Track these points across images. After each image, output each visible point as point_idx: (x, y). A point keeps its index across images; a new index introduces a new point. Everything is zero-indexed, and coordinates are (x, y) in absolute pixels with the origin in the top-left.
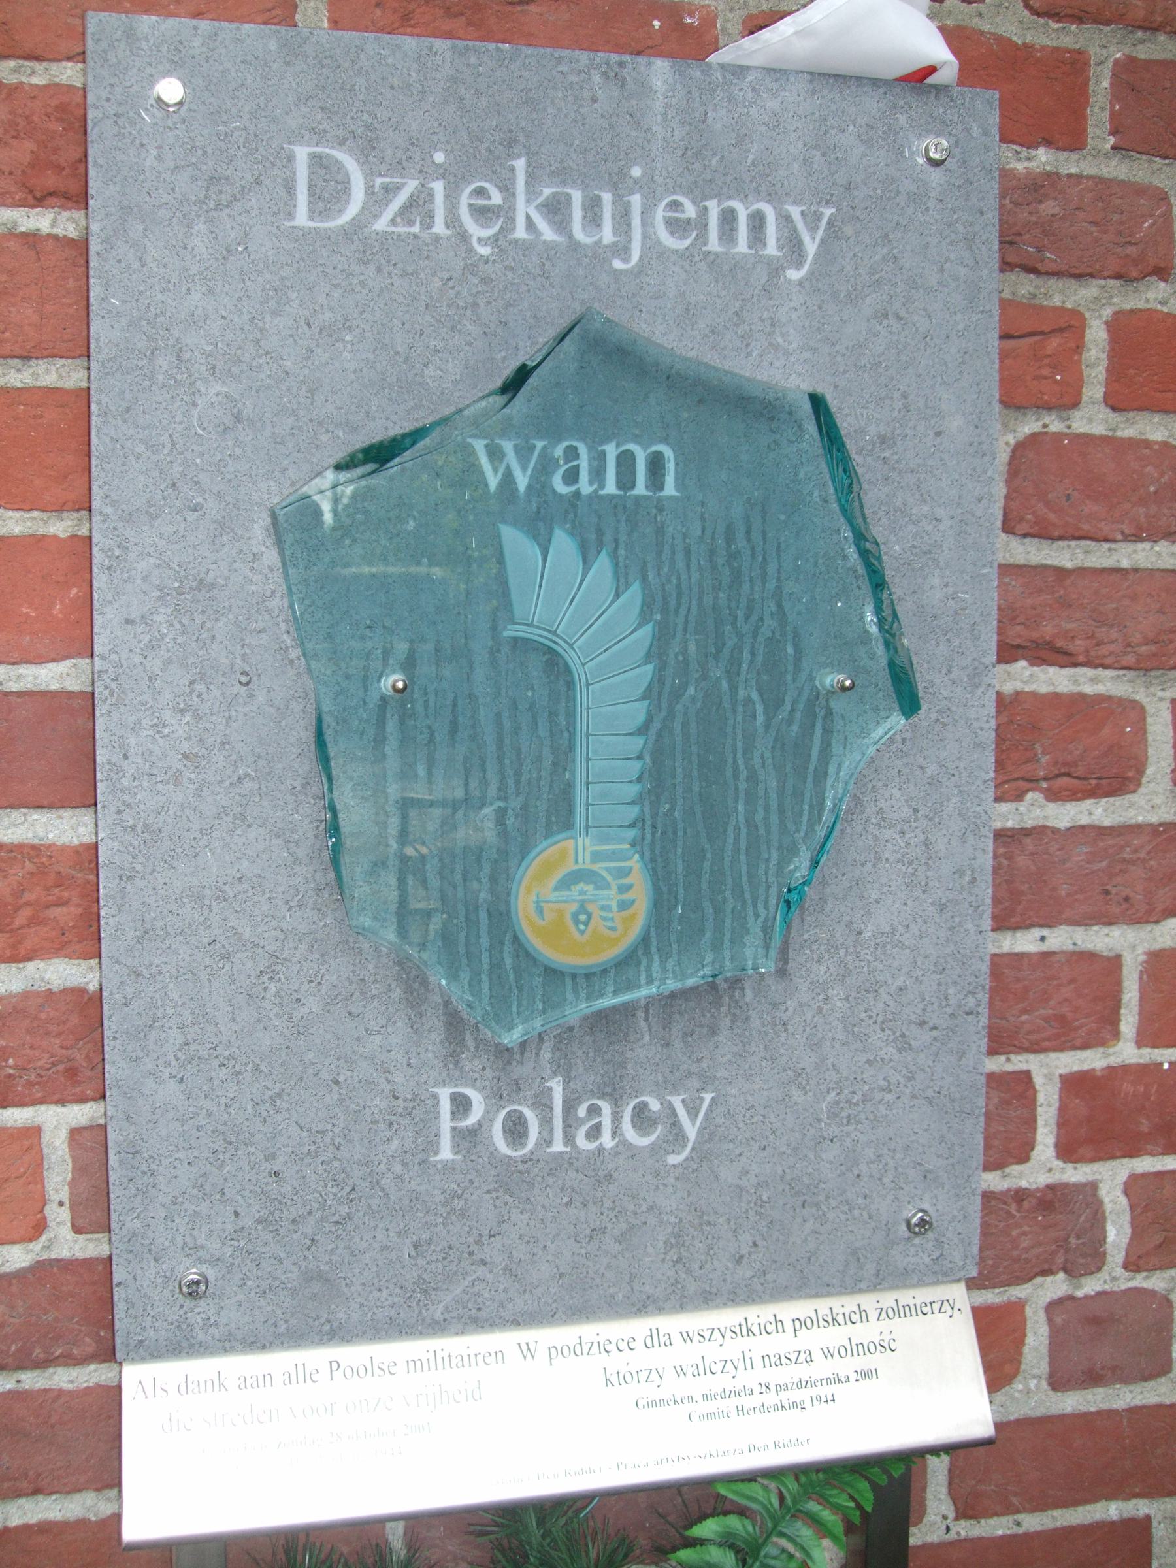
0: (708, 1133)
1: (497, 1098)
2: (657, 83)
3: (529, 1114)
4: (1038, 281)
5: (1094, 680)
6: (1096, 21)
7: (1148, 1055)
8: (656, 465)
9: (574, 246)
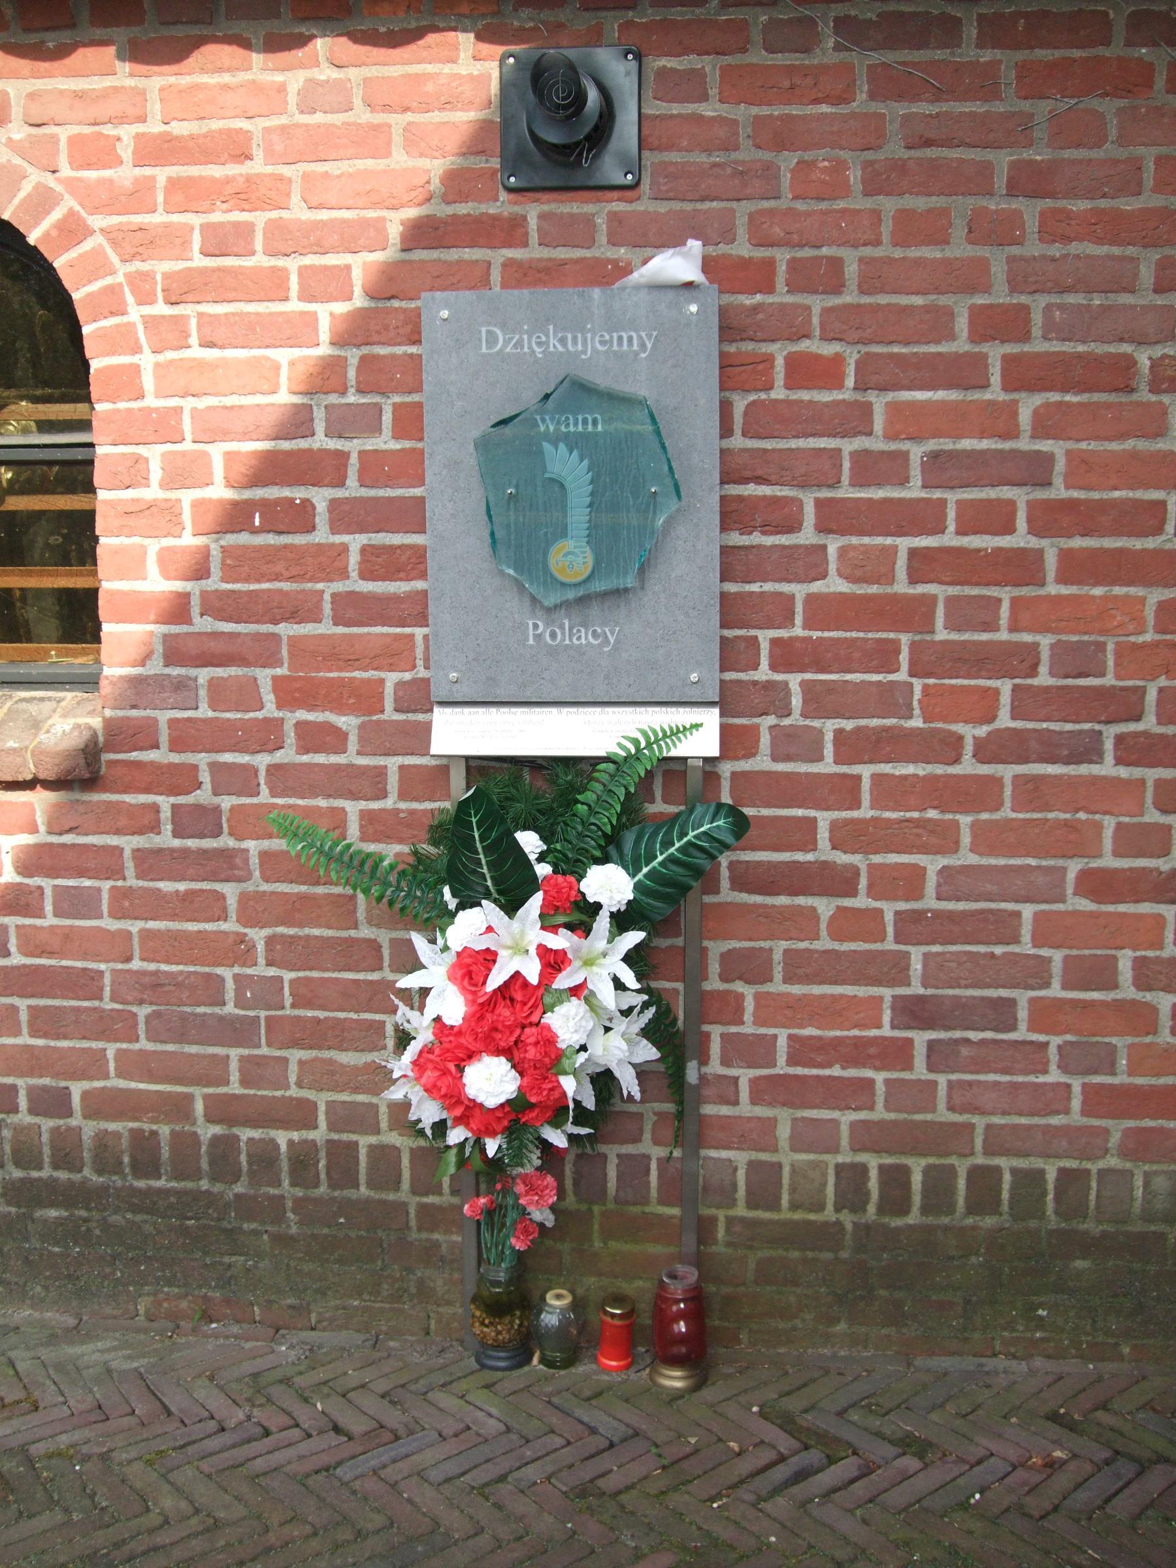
0: (617, 641)
1: (547, 625)
7: (807, 633)
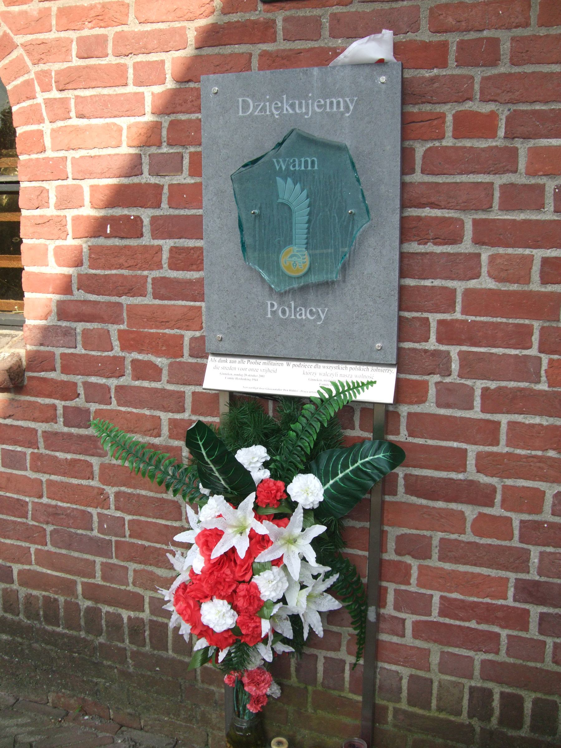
0: (326, 318)
1: (280, 304)
2: (315, 73)
3: (287, 309)
4: (432, 105)
5: (448, 213)
6: (450, 32)
7: (464, 317)
8: (313, 162)
9: (296, 114)
